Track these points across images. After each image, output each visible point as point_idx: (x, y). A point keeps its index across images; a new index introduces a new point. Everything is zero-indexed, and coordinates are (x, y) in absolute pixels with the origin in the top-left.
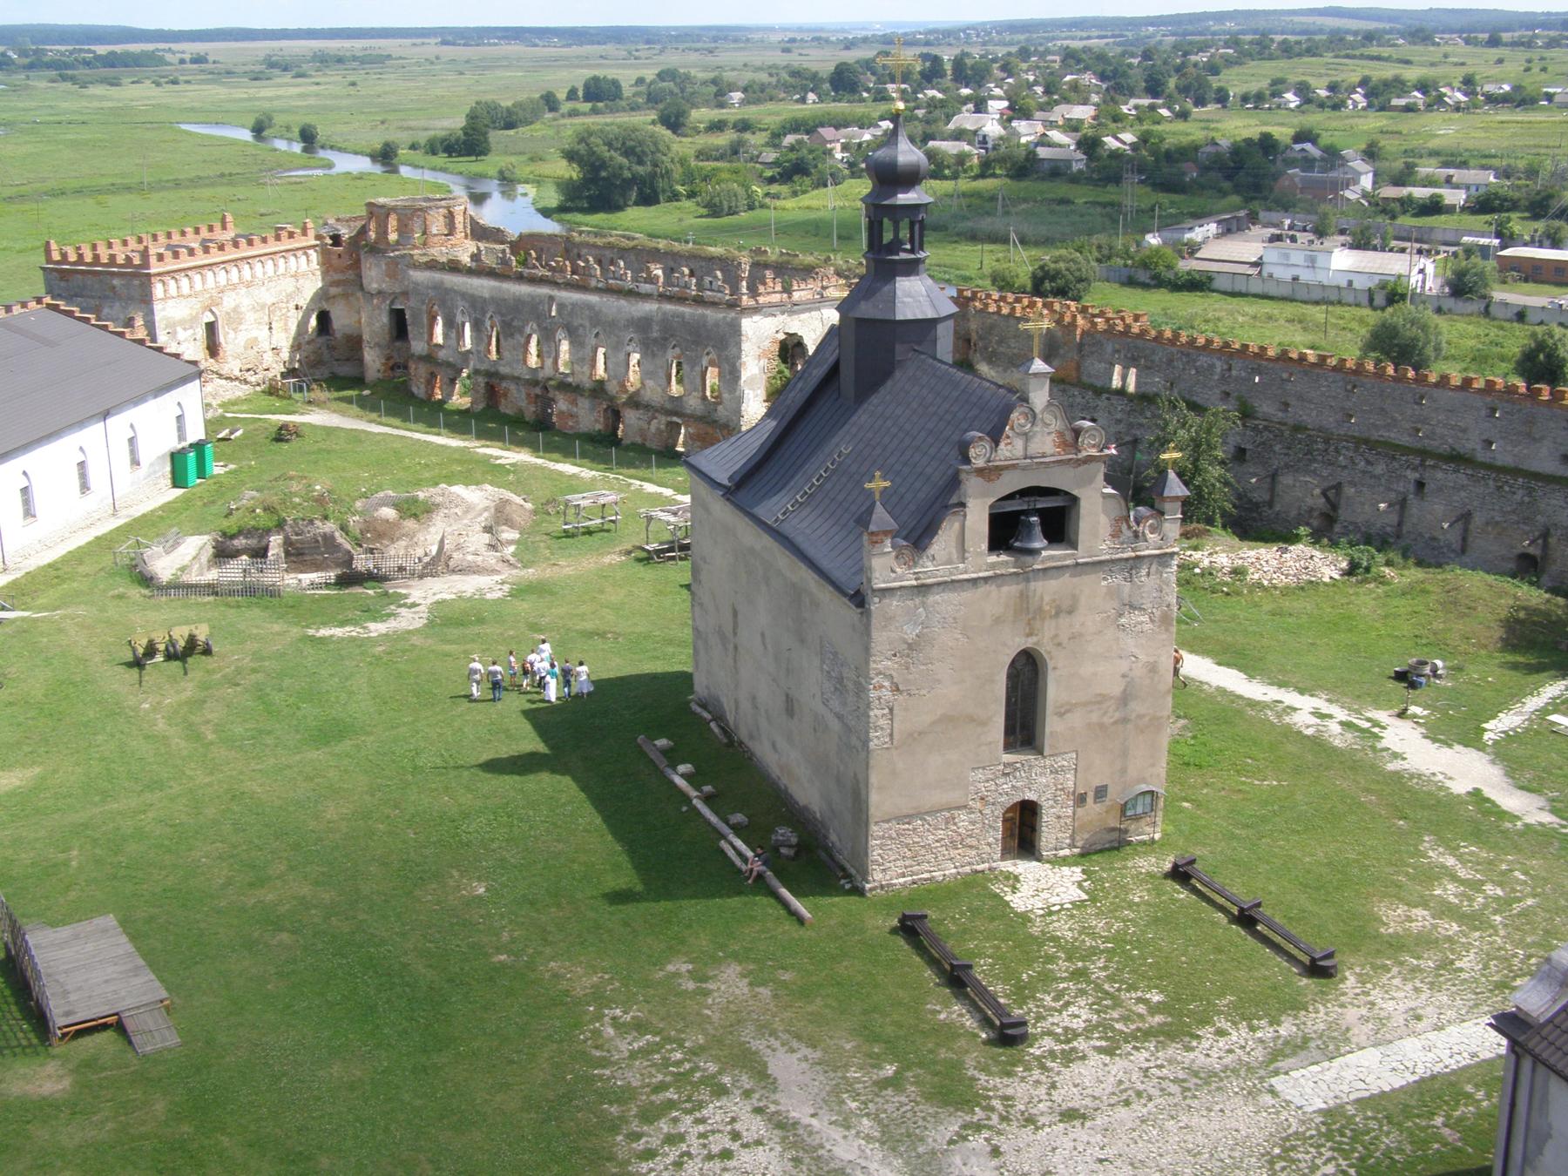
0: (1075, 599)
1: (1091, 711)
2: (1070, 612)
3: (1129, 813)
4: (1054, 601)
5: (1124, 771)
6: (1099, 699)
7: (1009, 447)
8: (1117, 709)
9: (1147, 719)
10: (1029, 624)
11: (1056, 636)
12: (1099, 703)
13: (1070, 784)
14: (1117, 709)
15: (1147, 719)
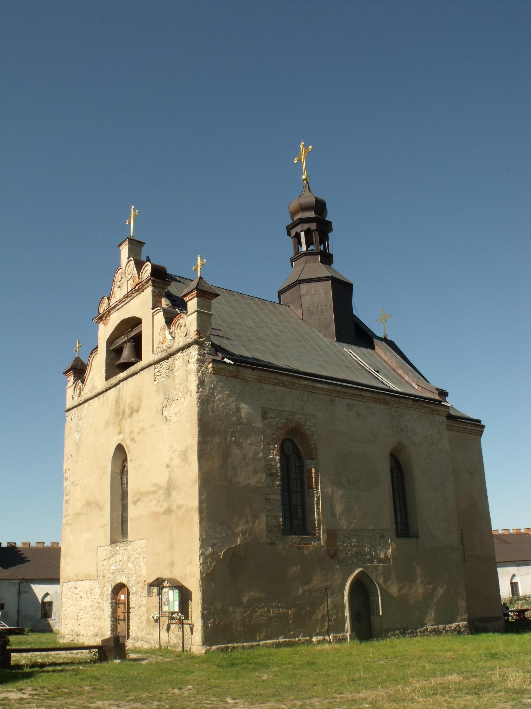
0: (140, 398)
1: (150, 501)
2: (137, 411)
3: (165, 608)
4: (130, 404)
5: (172, 564)
6: (154, 489)
7: (114, 298)
8: (164, 500)
9: (183, 510)
10: (119, 424)
11: (132, 432)
12: (154, 492)
13: (144, 571)
14: (164, 500)
15: (183, 510)
